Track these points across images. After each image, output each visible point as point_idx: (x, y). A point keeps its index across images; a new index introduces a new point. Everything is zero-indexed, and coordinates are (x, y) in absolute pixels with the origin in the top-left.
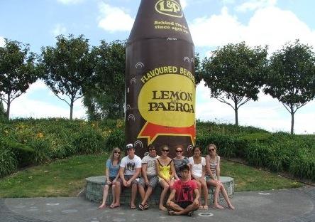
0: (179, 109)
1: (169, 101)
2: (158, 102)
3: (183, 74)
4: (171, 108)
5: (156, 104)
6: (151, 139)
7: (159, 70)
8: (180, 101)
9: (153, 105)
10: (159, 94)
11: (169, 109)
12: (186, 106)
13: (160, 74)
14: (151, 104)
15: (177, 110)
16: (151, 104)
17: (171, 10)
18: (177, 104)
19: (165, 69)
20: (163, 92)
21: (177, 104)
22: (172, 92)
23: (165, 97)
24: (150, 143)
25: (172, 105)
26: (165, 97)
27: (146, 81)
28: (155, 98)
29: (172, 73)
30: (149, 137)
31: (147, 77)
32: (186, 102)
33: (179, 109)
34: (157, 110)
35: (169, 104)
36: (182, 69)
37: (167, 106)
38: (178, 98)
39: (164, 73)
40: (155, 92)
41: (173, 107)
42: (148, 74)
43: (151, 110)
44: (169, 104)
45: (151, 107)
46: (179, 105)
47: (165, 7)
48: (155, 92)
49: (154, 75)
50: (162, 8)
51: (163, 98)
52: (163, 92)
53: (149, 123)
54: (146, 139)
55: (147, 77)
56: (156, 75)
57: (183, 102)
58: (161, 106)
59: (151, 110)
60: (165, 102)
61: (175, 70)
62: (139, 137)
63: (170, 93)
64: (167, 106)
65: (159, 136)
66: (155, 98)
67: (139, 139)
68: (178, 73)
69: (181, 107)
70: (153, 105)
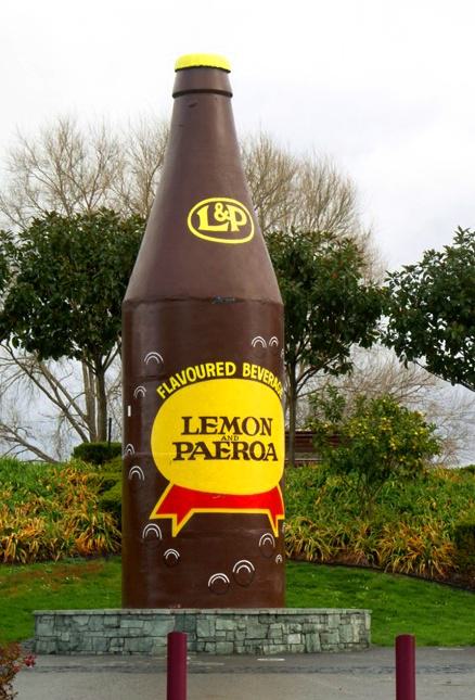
0: (241, 455)
1: (218, 438)
3: (249, 378)
4: (223, 455)
6: (179, 520)
7: (196, 371)
8: (243, 438)
9: (184, 448)
10: (195, 425)
11: (218, 456)
12: (258, 447)
13: (198, 380)
14: (178, 445)
15: (236, 457)
16: (178, 445)
17: (223, 228)
18: (236, 444)
19: (210, 368)
20: (203, 419)
21: (236, 444)
22: (225, 419)
23: (209, 429)
24: (176, 529)
25: (223, 446)
26: (209, 429)
27: (167, 395)
28: (186, 432)
29: (225, 377)
30: (174, 517)
31: (170, 387)
32: (258, 437)
33: (241, 455)
34: (192, 458)
35: (218, 444)
36: (246, 366)
37: (212, 450)
38: (237, 432)
39: (206, 378)
40: (187, 420)
41: (226, 451)
42: (172, 379)
43: (179, 458)
45: (179, 451)
46: (240, 447)
47: (212, 221)
48: (187, 420)
49: (184, 382)
50: (204, 225)
51: (204, 432)
52: (203, 419)
53: (175, 488)
54: (170, 521)
55: (170, 387)
56: (189, 383)
57: (250, 440)
58: (200, 450)
59: (179, 458)
62: (154, 516)
63: (221, 422)
64: (212, 450)
65: (196, 515)
67: (155, 521)
68: (239, 375)
70: (184, 448)
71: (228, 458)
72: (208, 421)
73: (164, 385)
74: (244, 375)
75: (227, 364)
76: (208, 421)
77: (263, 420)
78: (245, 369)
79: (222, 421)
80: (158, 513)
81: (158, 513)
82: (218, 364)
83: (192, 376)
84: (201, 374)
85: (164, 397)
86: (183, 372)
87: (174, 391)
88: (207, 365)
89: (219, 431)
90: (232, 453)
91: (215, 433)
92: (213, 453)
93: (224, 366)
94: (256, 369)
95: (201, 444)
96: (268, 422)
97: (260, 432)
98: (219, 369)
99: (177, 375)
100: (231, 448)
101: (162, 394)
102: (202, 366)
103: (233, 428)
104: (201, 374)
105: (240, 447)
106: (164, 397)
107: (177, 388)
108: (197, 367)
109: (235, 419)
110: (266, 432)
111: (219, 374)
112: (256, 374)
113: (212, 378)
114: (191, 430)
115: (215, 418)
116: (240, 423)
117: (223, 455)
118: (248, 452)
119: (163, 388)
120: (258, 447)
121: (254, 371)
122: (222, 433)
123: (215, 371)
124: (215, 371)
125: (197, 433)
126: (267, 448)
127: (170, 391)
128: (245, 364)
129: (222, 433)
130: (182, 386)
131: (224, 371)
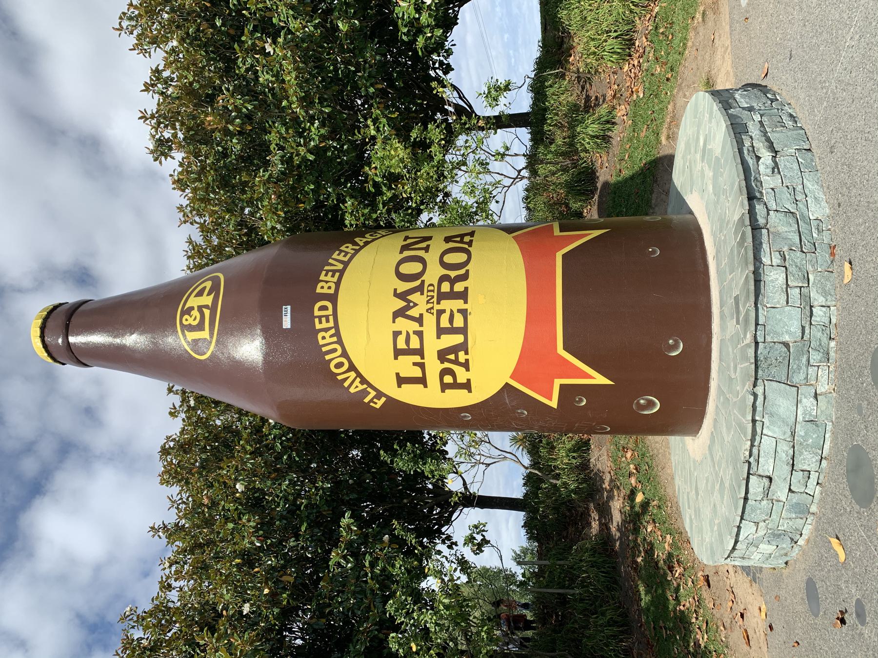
0: (459, 287)
2: (434, 367)
3: (338, 284)
4: (459, 322)
5: (444, 372)
7: (334, 358)
9: (448, 379)
11: (464, 331)
12: (449, 259)
13: (345, 354)
14: (444, 387)
15: (463, 295)
20: (398, 353)
21: (442, 296)
22: (397, 314)
23: (415, 343)
27: (379, 394)
28: (422, 381)
33: (459, 287)
34: (466, 365)
35: (441, 332)
38: (420, 289)
39: (340, 342)
42: (352, 390)
44: (441, 332)
46: (446, 287)
49: (353, 375)
51: (420, 352)
52: (398, 353)
53: (512, 377)
60: (433, 345)
61: (324, 308)
66: (422, 381)
68: (333, 298)
69: (453, 281)
70: (448, 379)
71: (464, 312)
72: (401, 345)
73: (366, 400)
74: (332, 291)
75: (317, 313)
76: (401, 345)
77: (404, 248)
78: (325, 291)
79: (400, 320)
80: (550, 399)
81: (550, 399)
82: (318, 326)
83: (339, 365)
84: (335, 350)
85: (383, 399)
86: (340, 378)
87: (370, 385)
88: (321, 342)
89: (415, 326)
90: (459, 304)
91: (420, 334)
92: (457, 339)
93: (320, 317)
94: (328, 271)
95: (442, 355)
96: (409, 241)
97: (421, 253)
98: (325, 325)
99: (346, 384)
100: (446, 305)
101: (379, 403)
102: (324, 349)
103: (415, 297)
104: (335, 350)
105: (446, 287)
106: (383, 399)
107: (364, 381)
108: (327, 357)
109: (396, 295)
110: (424, 245)
111: (331, 324)
112: (334, 272)
113: (338, 334)
114: (417, 373)
115: (396, 334)
116: (404, 286)
117: (459, 322)
118: (453, 274)
119: (371, 401)
120: (450, 259)
121: (329, 278)
122: (420, 320)
123: (326, 330)
124: (326, 330)
125: (422, 366)
126: (451, 245)
127: (373, 393)
128: (319, 290)
129: (420, 320)
130: (359, 375)
131: (327, 317)
